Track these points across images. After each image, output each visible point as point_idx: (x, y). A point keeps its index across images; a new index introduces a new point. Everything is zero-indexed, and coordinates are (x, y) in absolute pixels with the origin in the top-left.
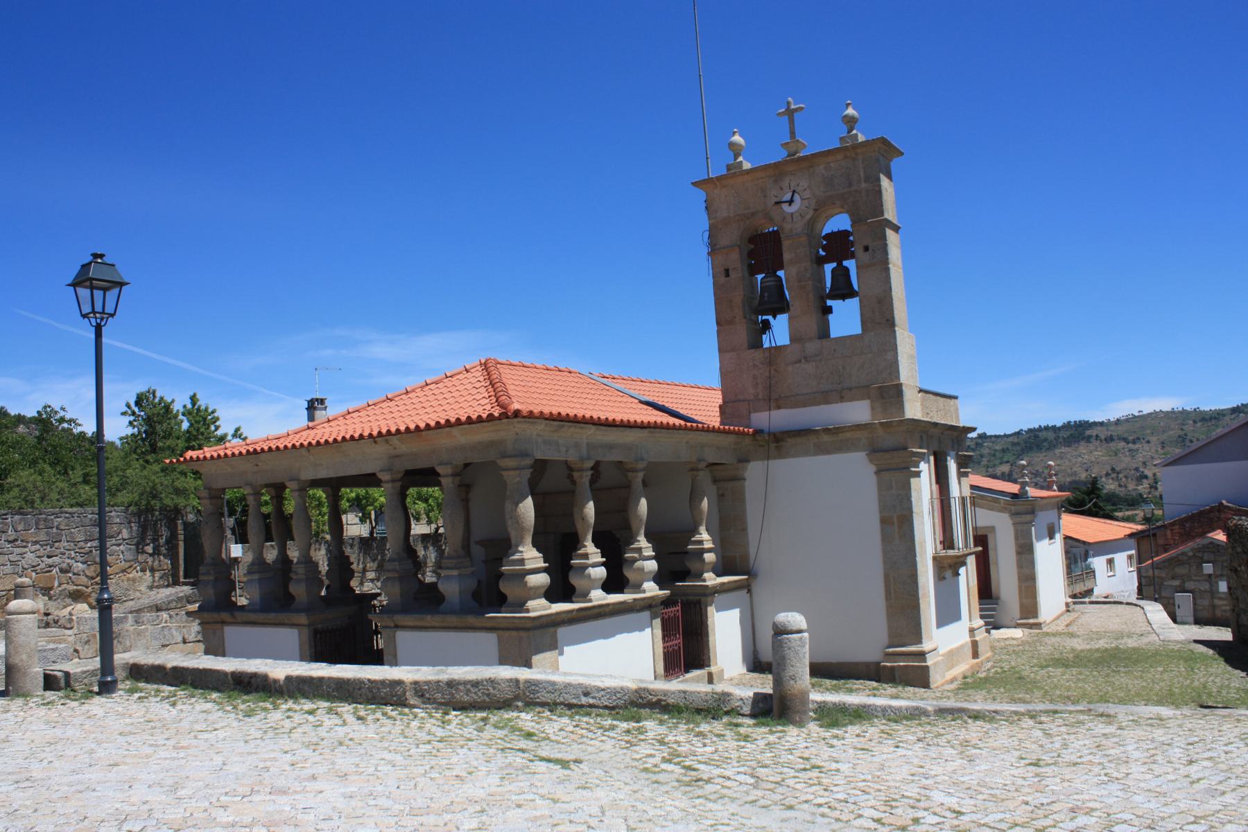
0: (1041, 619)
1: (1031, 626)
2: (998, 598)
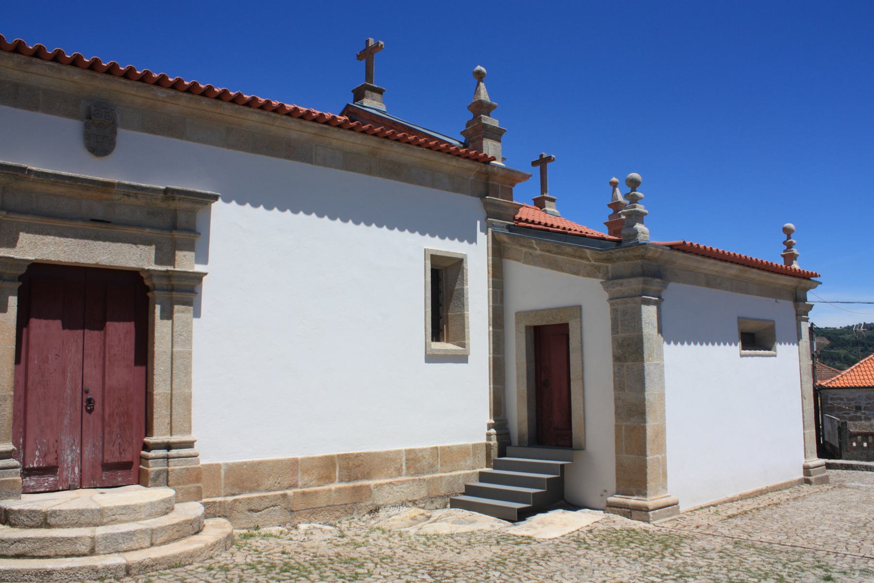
0: (650, 501)
1: (630, 512)
2: (581, 448)
